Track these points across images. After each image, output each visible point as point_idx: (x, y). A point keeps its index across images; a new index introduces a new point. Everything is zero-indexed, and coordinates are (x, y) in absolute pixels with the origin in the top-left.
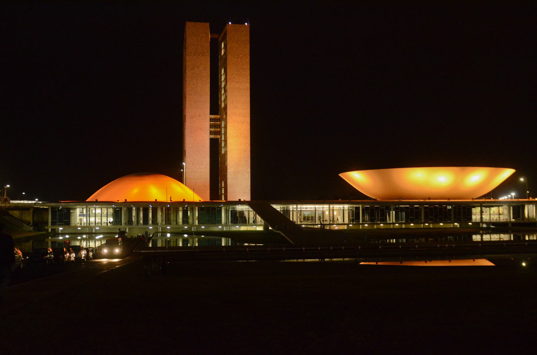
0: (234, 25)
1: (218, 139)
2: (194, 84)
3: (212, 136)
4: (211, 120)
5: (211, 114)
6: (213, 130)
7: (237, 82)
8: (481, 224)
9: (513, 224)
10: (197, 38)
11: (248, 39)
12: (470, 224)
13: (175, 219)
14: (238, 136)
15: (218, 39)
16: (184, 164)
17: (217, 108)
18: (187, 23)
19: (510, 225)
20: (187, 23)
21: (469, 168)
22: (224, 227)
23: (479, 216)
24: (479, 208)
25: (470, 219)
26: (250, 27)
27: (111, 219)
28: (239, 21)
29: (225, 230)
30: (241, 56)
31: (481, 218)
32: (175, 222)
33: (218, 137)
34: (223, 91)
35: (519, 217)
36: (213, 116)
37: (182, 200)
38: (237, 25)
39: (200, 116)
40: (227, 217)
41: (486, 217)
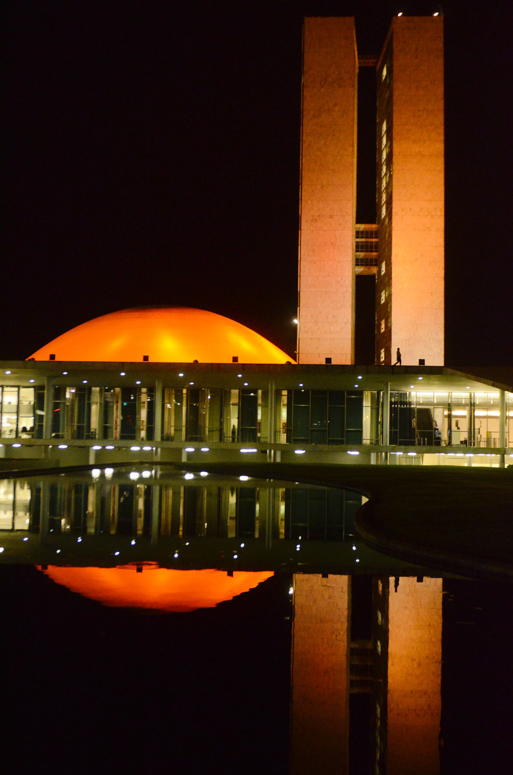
0: (410, 18)
1: (374, 276)
3: (360, 270)
4: (358, 234)
5: (359, 220)
6: (362, 255)
7: (414, 141)
10: (330, 55)
11: (441, 45)
13: (217, 425)
15: (375, 67)
16: (296, 321)
17: (370, 206)
20: (307, 20)
22: (373, 456)
26: (446, 21)
27: (28, 422)
28: (419, 8)
29: (373, 462)
32: (216, 435)
33: (374, 270)
34: (384, 168)
36: (362, 227)
38: (416, 19)
39: (331, 217)
40: (377, 423)
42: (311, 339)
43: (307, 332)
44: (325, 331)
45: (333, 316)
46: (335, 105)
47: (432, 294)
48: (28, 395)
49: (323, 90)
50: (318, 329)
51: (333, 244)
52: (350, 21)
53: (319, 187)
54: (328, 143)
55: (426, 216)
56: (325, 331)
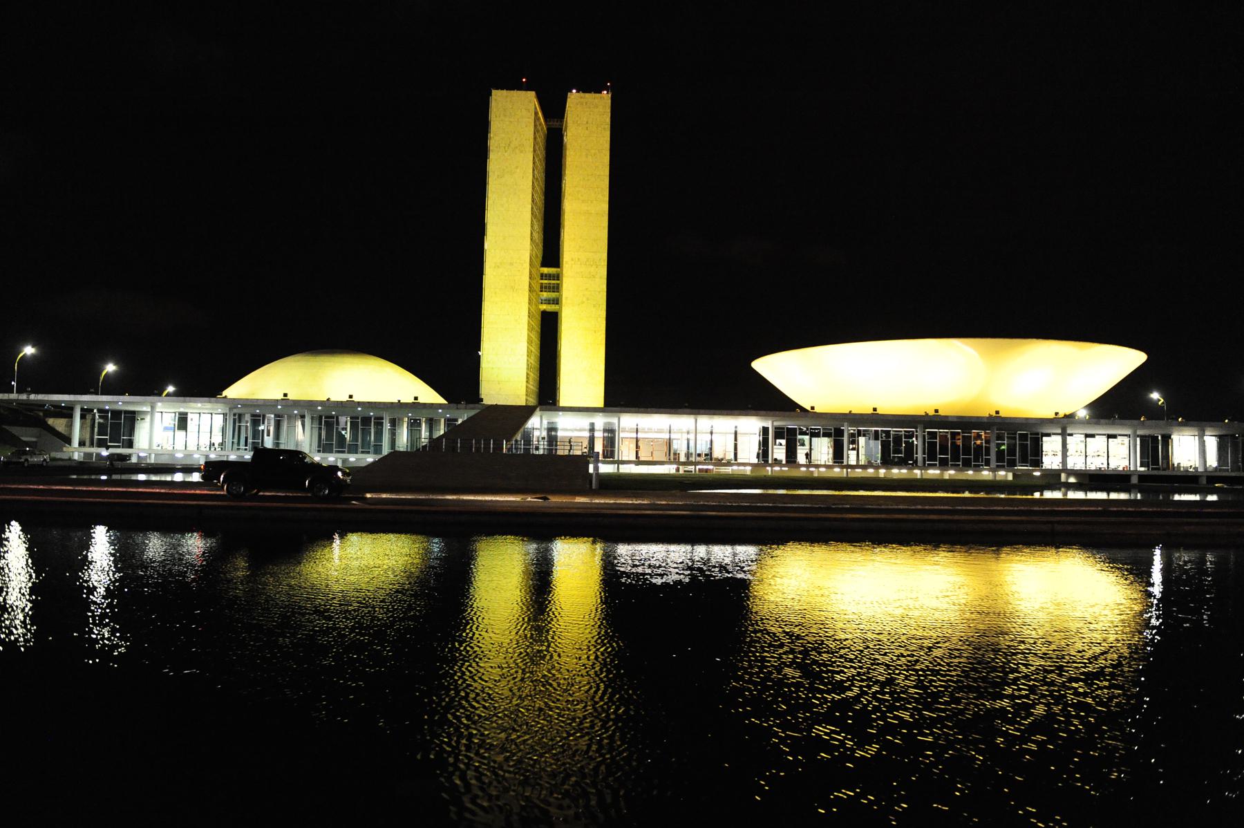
3: (544, 307)
8: (1063, 476)
9: (1142, 477)
12: (1037, 474)
17: (550, 251)
18: (494, 92)
19: (1134, 480)
20: (494, 92)
21: (1034, 340)
23: (1059, 458)
24: (1059, 438)
25: (1038, 463)
27: (217, 439)
31: (1064, 462)
35: (1155, 461)
36: (546, 270)
37: (346, 398)
39: (511, 264)
41: (1076, 462)
48: (219, 420)
51: (513, 288)
52: (531, 95)
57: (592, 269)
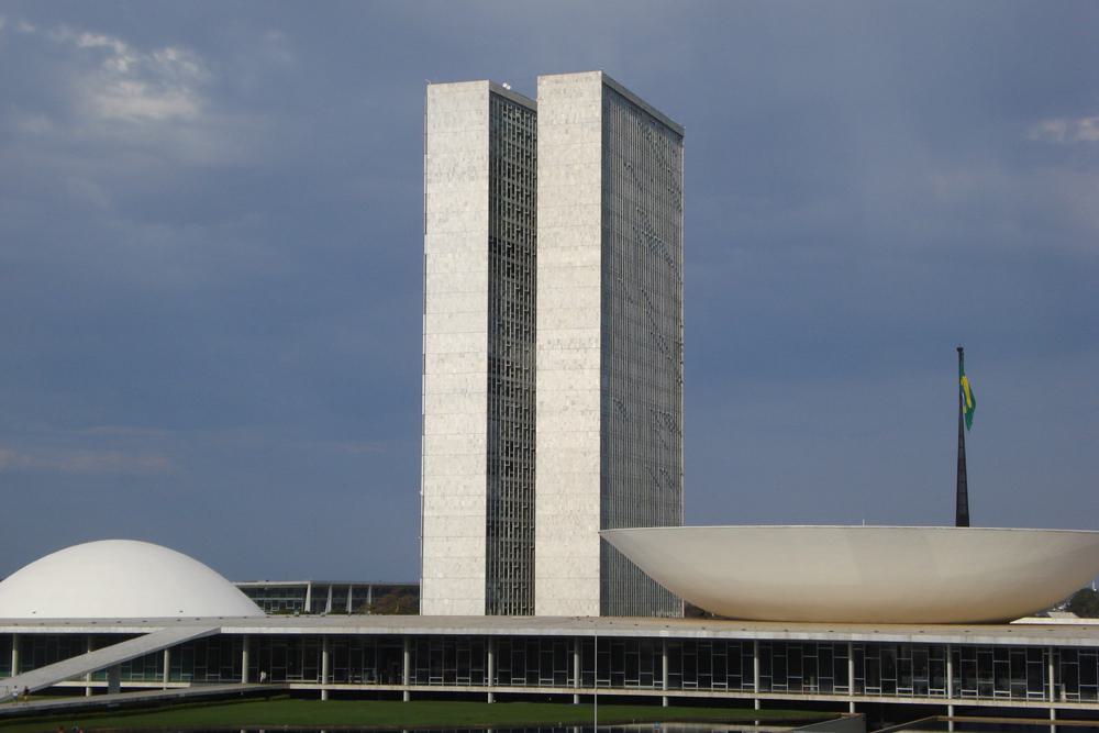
0: (559, 77)
2: (447, 265)
7: (563, 248)
14: (566, 409)
18: (430, 88)
20: (430, 88)
30: (576, 167)
39: (462, 355)
42: (438, 517)
43: (433, 508)
44: (455, 508)
45: (465, 487)
46: (466, 204)
47: (585, 454)
49: (450, 185)
50: (446, 504)
51: (464, 392)
53: (447, 316)
54: (457, 256)
55: (578, 350)
56: (455, 508)
57: (578, 356)
